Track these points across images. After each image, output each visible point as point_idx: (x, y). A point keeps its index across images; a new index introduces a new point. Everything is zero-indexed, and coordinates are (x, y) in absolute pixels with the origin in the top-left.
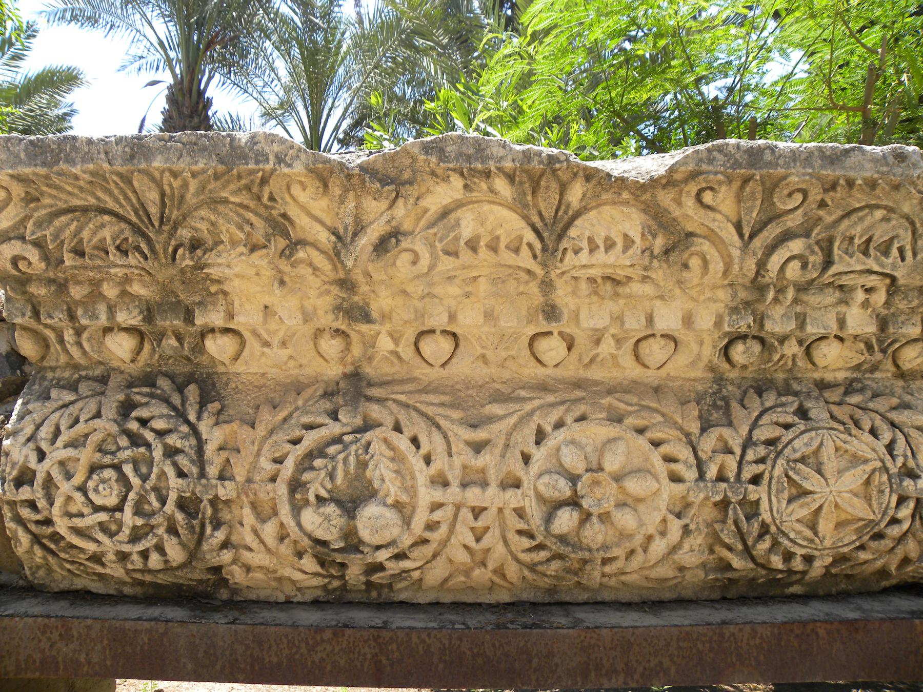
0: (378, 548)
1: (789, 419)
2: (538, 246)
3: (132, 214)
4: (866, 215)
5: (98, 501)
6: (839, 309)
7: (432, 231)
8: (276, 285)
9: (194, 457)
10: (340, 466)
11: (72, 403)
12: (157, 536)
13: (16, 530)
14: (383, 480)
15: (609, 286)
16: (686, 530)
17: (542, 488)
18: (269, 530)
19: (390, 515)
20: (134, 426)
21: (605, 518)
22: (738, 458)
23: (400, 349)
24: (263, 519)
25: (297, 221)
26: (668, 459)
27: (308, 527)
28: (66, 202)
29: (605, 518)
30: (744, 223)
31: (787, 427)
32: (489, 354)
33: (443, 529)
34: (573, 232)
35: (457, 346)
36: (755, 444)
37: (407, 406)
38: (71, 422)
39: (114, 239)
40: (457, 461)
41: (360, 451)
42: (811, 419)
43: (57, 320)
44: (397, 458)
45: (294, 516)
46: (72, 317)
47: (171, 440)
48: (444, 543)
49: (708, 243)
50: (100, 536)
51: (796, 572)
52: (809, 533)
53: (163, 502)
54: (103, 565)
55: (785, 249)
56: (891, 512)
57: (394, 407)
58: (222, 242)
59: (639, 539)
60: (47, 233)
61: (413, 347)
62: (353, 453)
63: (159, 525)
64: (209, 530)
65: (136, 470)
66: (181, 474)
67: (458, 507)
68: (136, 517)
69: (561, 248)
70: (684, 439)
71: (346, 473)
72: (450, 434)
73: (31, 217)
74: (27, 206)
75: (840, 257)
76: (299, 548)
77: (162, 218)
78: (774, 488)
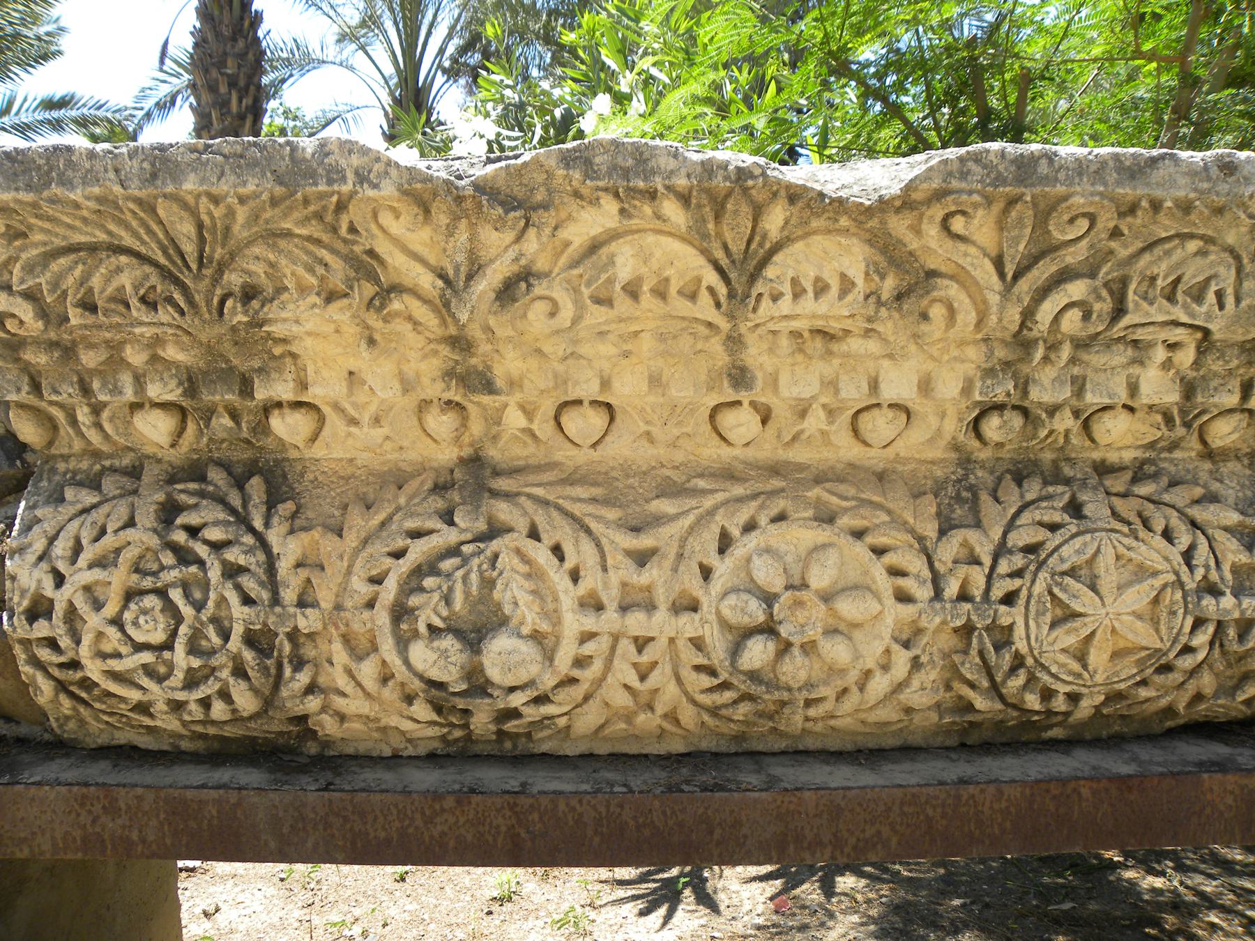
0: (512, 689)
1: (1057, 517)
2: (722, 290)
3: (159, 253)
4: (1175, 248)
5: (139, 637)
6: (1131, 371)
7: (575, 272)
8: (364, 345)
9: (264, 578)
10: (459, 587)
11: (94, 506)
12: (221, 680)
13: (34, 676)
14: (516, 604)
15: (818, 343)
16: (916, 664)
17: (726, 612)
18: (368, 671)
19: (527, 649)
20: (180, 537)
21: (809, 648)
22: (987, 571)
23: (535, 427)
24: (358, 656)
25: (389, 260)
26: (895, 572)
27: (419, 666)
28: (65, 238)
29: (809, 648)
30: (1007, 259)
31: (1053, 527)
32: (655, 430)
33: (597, 667)
34: (770, 272)
35: (612, 419)
36: (1010, 552)
37: (545, 503)
38: (95, 533)
39: (136, 288)
40: (614, 578)
41: (485, 566)
42: (1085, 517)
43: (65, 396)
44: (535, 574)
45: (399, 652)
46: (86, 390)
47: (233, 555)
48: (599, 682)
49: (956, 286)
50: (145, 682)
51: (1057, 713)
52: (1076, 666)
53: (226, 637)
54: (151, 716)
55: (1062, 294)
56: (1184, 639)
57: (528, 505)
58: (286, 289)
59: (853, 676)
60: (42, 280)
61: (552, 422)
62: (475, 569)
63: (222, 667)
64: (288, 672)
65: (187, 595)
66: (247, 600)
67: (616, 638)
68: (191, 657)
69: (754, 293)
70: (917, 546)
71: (467, 594)
72: (604, 541)
73: (17, 259)
74: (10, 243)
75: (1136, 304)
76: (407, 690)
77: (201, 257)
78: (1033, 609)
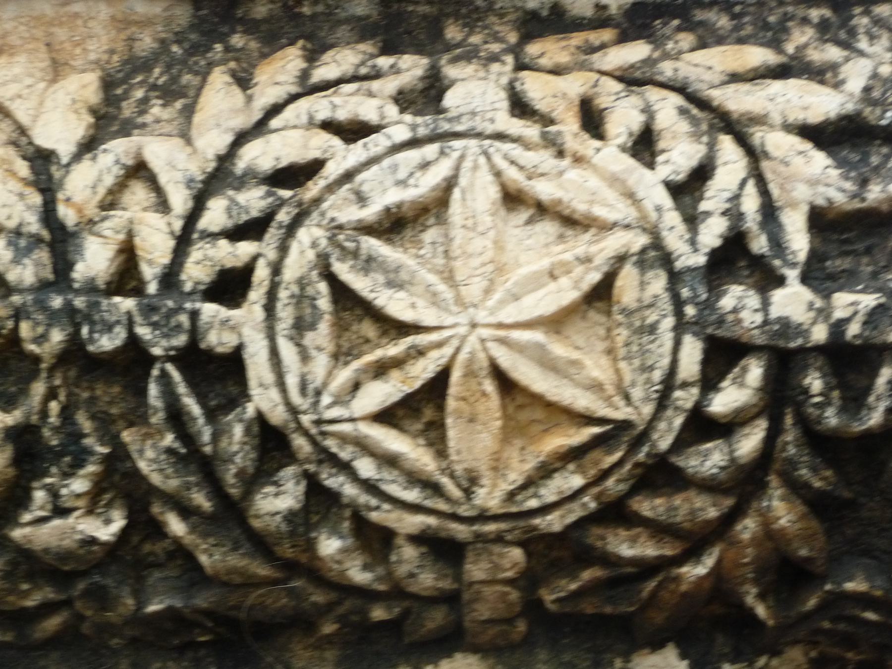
22: (178, 225)
56: (686, 398)
78: (285, 314)
